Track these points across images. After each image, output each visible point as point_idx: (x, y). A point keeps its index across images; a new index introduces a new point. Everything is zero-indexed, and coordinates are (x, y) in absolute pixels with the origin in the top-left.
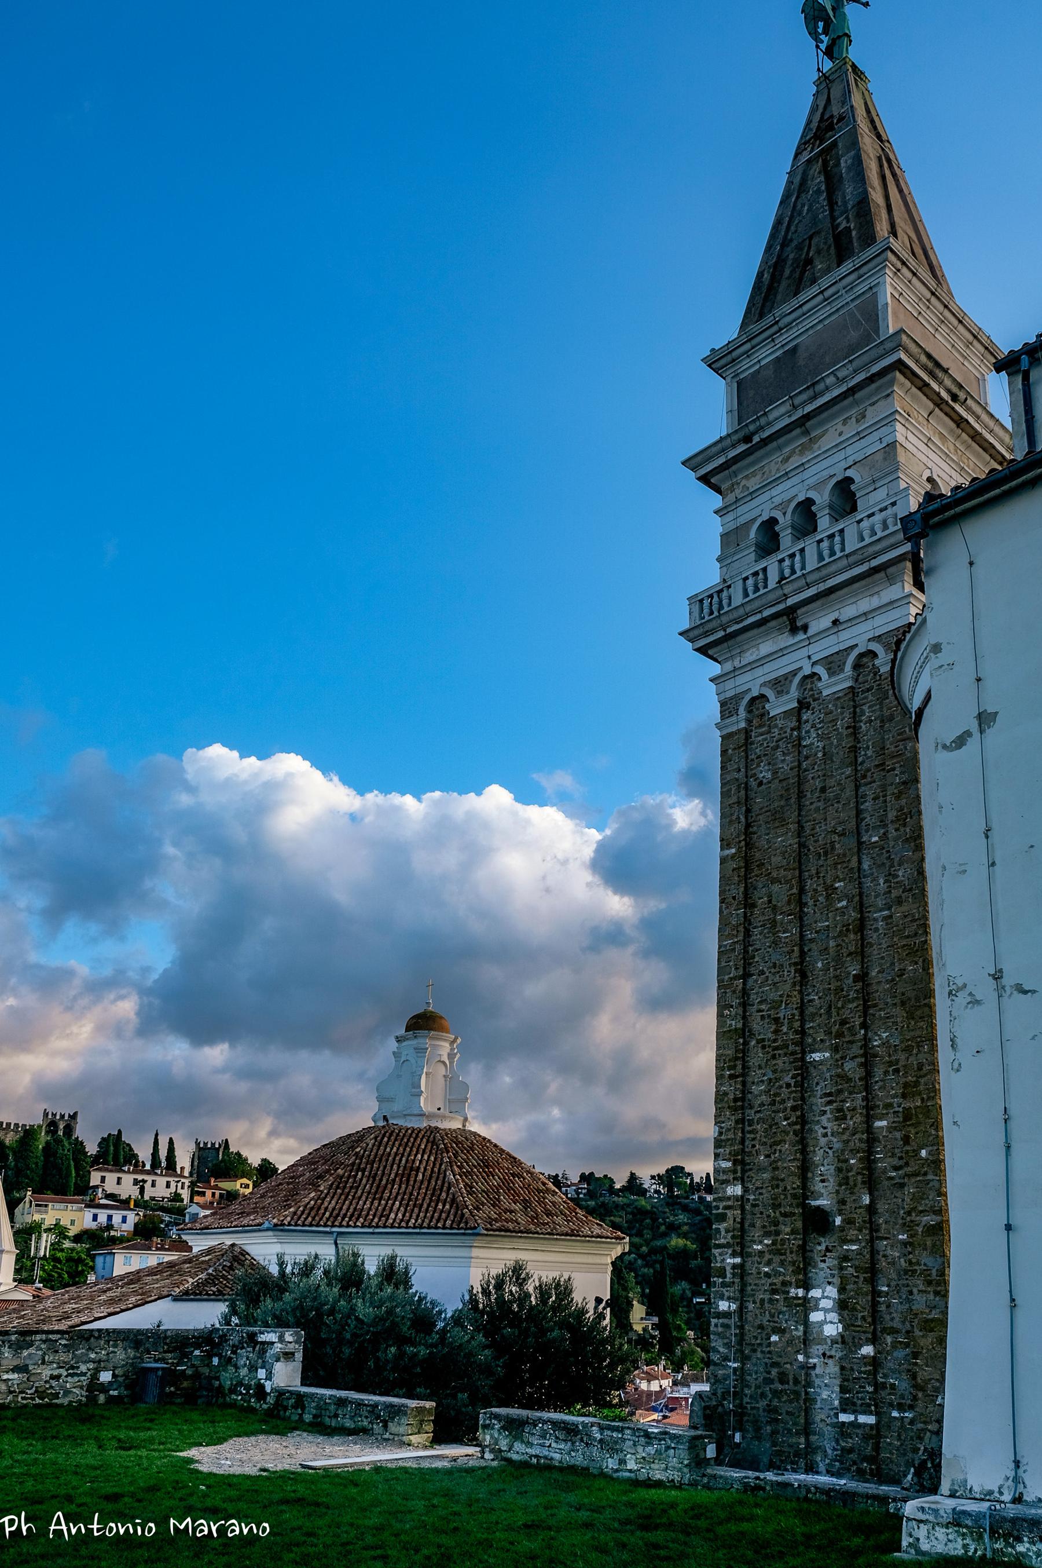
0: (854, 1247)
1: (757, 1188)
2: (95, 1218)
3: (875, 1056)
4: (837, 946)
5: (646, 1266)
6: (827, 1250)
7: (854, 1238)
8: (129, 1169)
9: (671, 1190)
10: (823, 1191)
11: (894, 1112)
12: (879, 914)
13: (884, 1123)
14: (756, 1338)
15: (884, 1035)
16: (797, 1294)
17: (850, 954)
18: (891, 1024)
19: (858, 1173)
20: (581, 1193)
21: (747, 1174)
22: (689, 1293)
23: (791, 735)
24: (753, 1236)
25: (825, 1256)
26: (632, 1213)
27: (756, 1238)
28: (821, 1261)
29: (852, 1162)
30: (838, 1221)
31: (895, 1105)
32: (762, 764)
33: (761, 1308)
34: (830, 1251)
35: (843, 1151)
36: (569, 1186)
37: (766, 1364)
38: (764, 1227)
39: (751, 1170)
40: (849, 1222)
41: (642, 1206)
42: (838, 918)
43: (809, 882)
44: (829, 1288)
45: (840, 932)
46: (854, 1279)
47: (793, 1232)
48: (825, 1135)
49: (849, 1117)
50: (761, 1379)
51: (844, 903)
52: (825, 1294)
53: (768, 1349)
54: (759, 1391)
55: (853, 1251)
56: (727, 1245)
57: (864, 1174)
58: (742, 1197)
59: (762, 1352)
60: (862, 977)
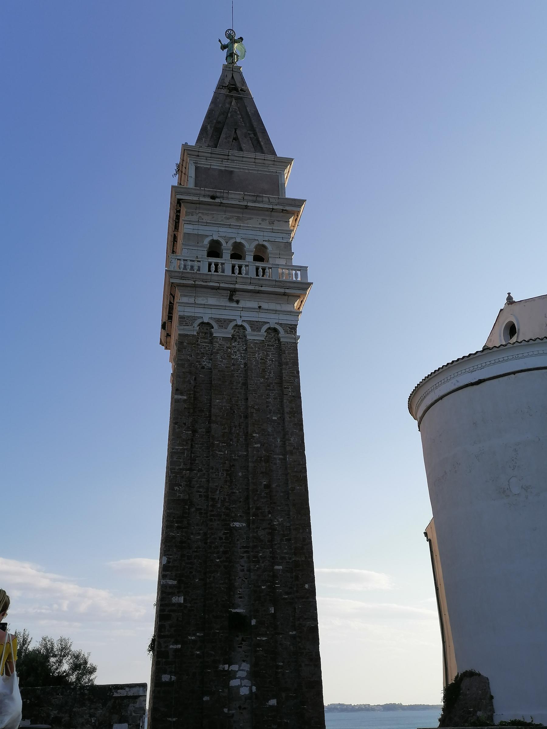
3: (276, 530)
4: (255, 467)
6: (243, 640)
11: (287, 562)
12: (278, 456)
13: (281, 567)
15: (280, 520)
16: (224, 668)
17: (262, 473)
25: (242, 644)
28: (239, 647)
30: (253, 622)
31: (287, 558)
32: (205, 358)
34: (245, 641)
42: (255, 452)
43: (234, 429)
44: (244, 664)
49: (261, 562)
51: (259, 445)
52: (241, 668)
60: (267, 486)
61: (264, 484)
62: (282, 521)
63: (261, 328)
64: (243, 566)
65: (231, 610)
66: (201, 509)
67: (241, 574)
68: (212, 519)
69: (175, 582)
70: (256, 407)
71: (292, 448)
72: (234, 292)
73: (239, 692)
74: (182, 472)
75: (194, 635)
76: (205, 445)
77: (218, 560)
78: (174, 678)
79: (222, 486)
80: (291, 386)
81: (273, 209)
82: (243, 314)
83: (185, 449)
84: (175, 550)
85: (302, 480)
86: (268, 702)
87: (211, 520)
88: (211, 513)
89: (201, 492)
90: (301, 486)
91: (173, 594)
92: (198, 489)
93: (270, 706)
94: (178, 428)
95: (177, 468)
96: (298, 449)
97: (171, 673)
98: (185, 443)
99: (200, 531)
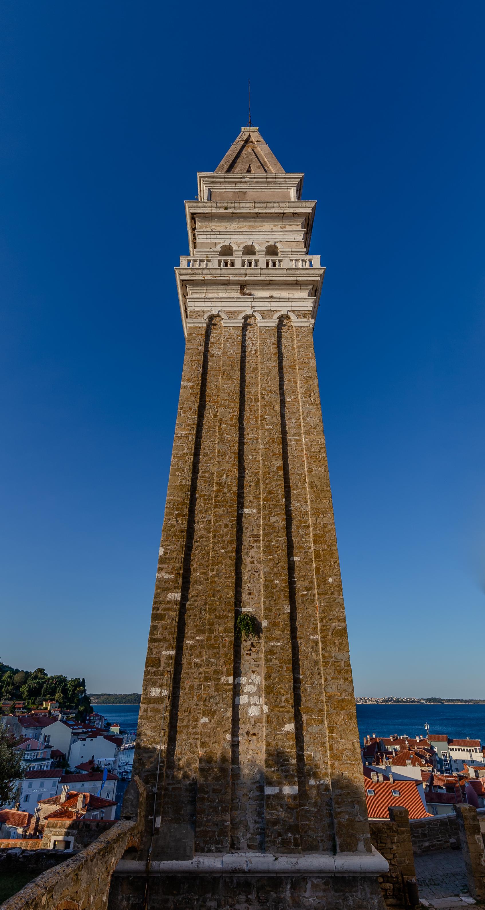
0: (279, 644)
7: (278, 637)
10: (249, 601)
12: (293, 437)
15: (297, 505)
16: (227, 681)
18: (301, 499)
19: (281, 590)
23: (237, 338)
25: (250, 650)
28: (247, 654)
29: (277, 582)
32: (214, 347)
35: (269, 574)
40: (273, 625)
45: (268, 441)
46: (278, 668)
47: (225, 631)
48: (252, 562)
51: (271, 427)
55: (277, 646)
57: (286, 591)
61: (277, 466)
62: (298, 506)
63: (272, 316)
64: (252, 558)
65: (238, 608)
67: (250, 566)
68: (217, 505)
69: (172, 577)
70: (267, 389)
71: (309, 428)
72: (245, 285)
73: (247, 713)
75: (193, 638)
77: (223, 551)
79: (229, 469)
80: (306, 367)
81: (284, 213)
82: (253, 304)
83: (189, 433)
85: (320, 461)
86: (283, 727)
90: (320, 467)
91: (168, 590)
93: (288, 733)
94: (183, 413)
95: (180, 452)
96: (315, 428)
97: (161, 686)
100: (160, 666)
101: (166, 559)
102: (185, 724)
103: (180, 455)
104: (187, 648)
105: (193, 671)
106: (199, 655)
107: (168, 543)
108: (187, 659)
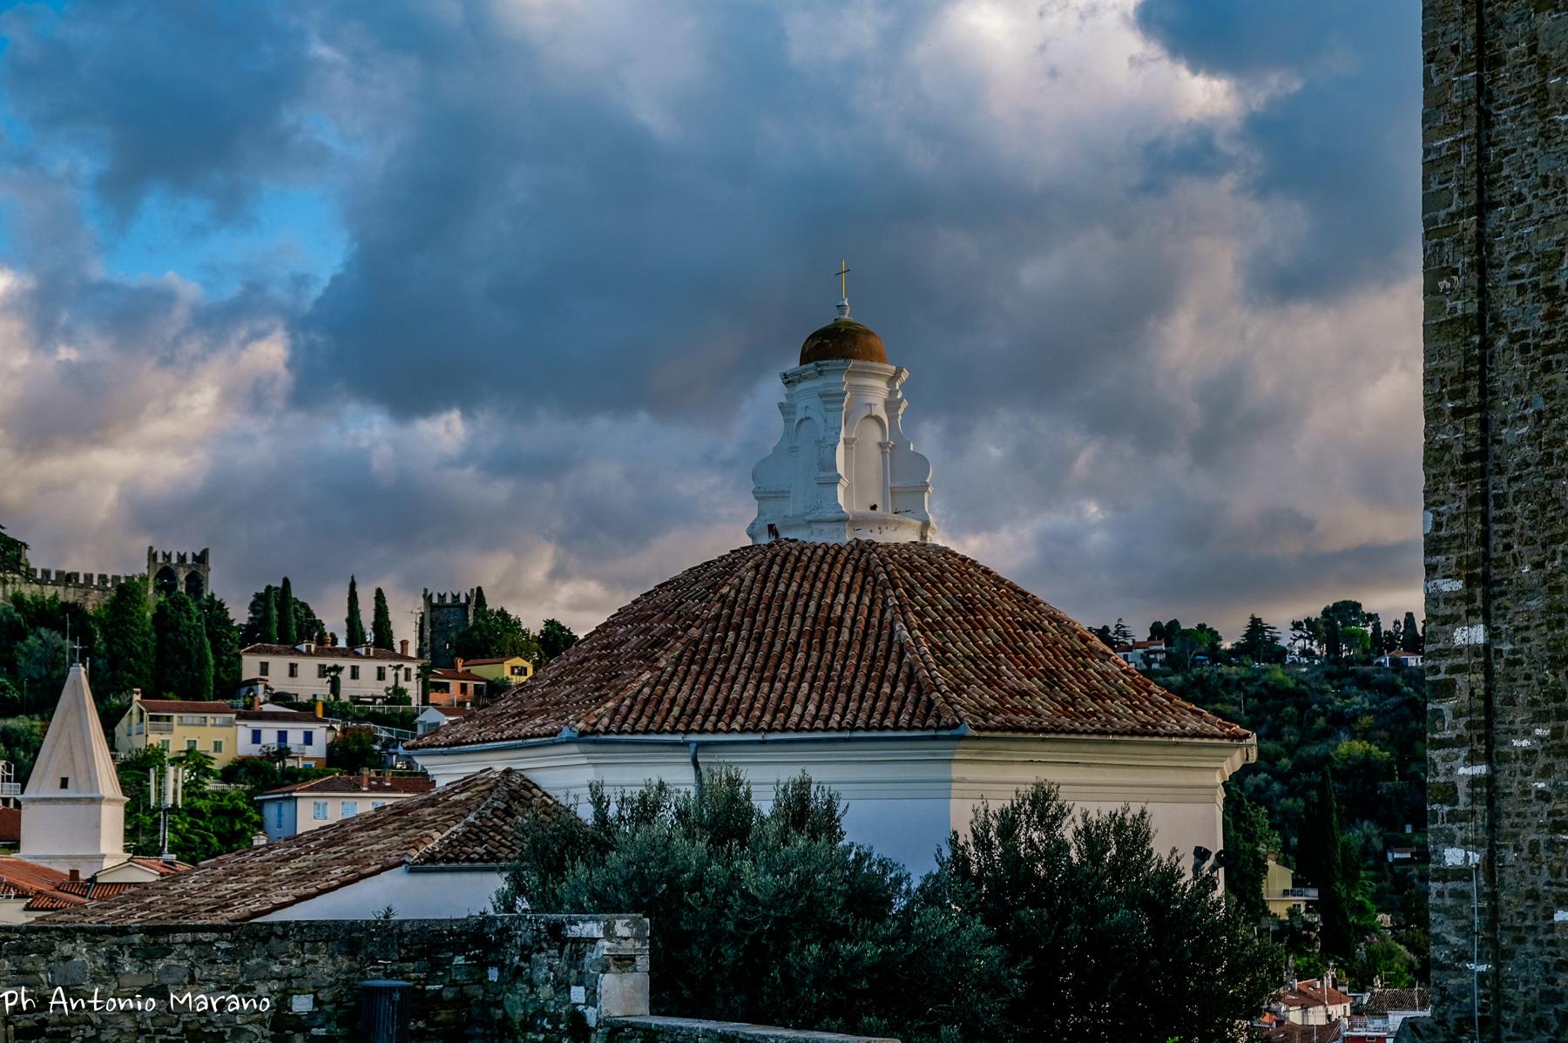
1: (1517, 630)
2: (256, 737)
5: (1289, 794)
8: (309, 648)
9: (1334, 648)
14: (1523, 916)
20: (1155, 660)
21: (1495, 603)
22: (1377, 843)
24: (1512, 723)
26: (1258, 695)
27: (1517, 726)
33: (1532, 860)
36: (1130, 649)
37: (1546, 965)
38: (1534, 703)
39: (1503, 594)
41: (1278, 681)
50: (1535, 995)
53: (1549, 937)
54: (1533, 1017)
56: (1459, 742)
58: (1487, 647)
59: (1538, 943)
66: (1524, 335)
68: (1550, 362)
69: (1458, 585)
74: (1457, 224)
75: (1528, 734)
76: (1529, 101)
78: (1475, 858)
83: (1460, 140)
84: (1451, 484)
87: (1547, 367)
88: (1546, 342)
89: (1522, 276)
91: (1453, 620)
92: (1515, 268)
95: (1442, 214)
97: (1465, 843)
98: (1458, 120)
99: (1524, 409)
100: (1456, 802)
101: (1440, 540)
102: (1528, 923)
103: (1443, 222)
104: (1517, 758)
105: (1536, 808)
106: (1545, 773)
107: (1440, 496)
108: (1519, 783)
